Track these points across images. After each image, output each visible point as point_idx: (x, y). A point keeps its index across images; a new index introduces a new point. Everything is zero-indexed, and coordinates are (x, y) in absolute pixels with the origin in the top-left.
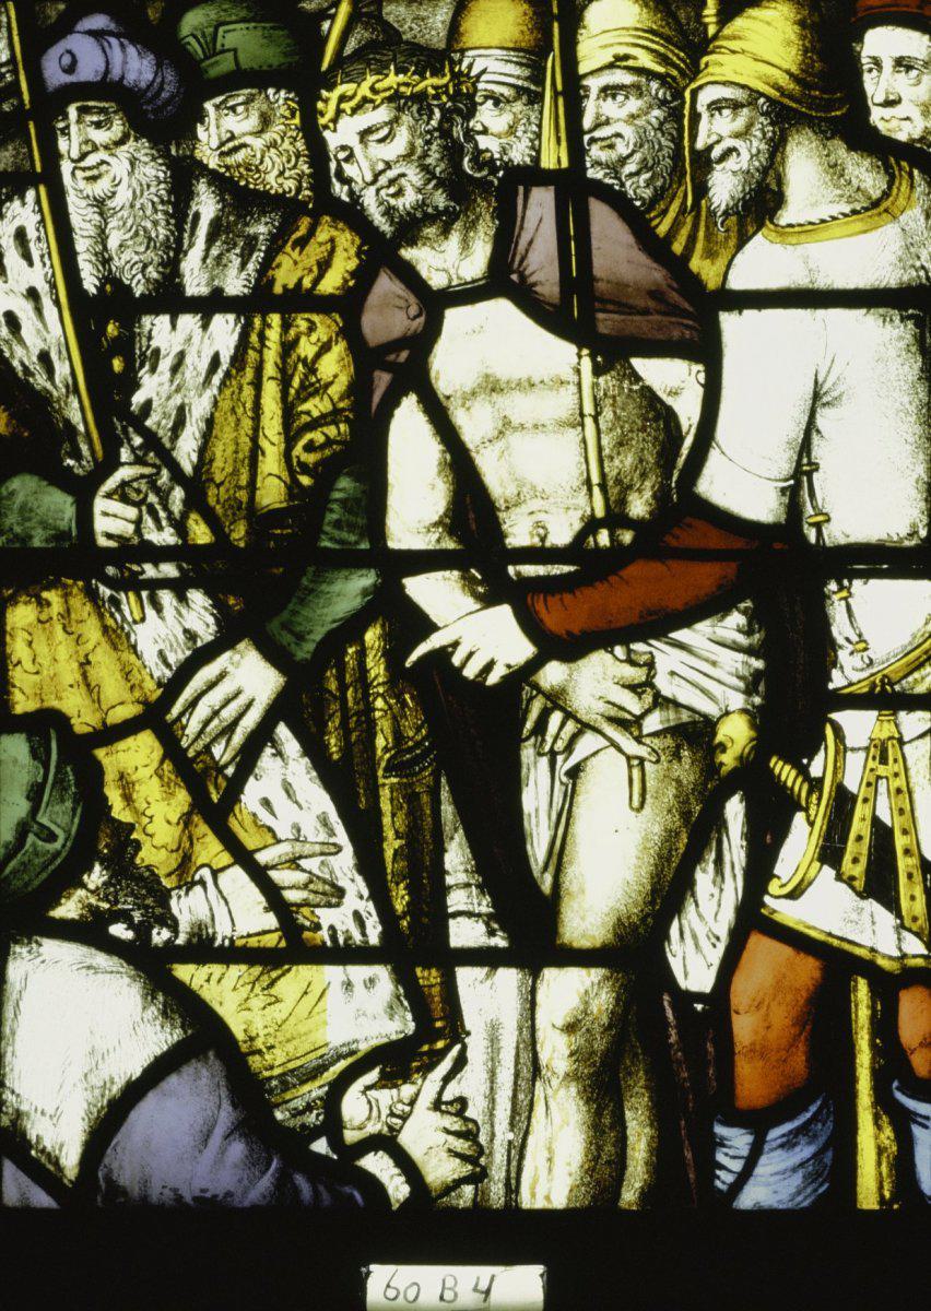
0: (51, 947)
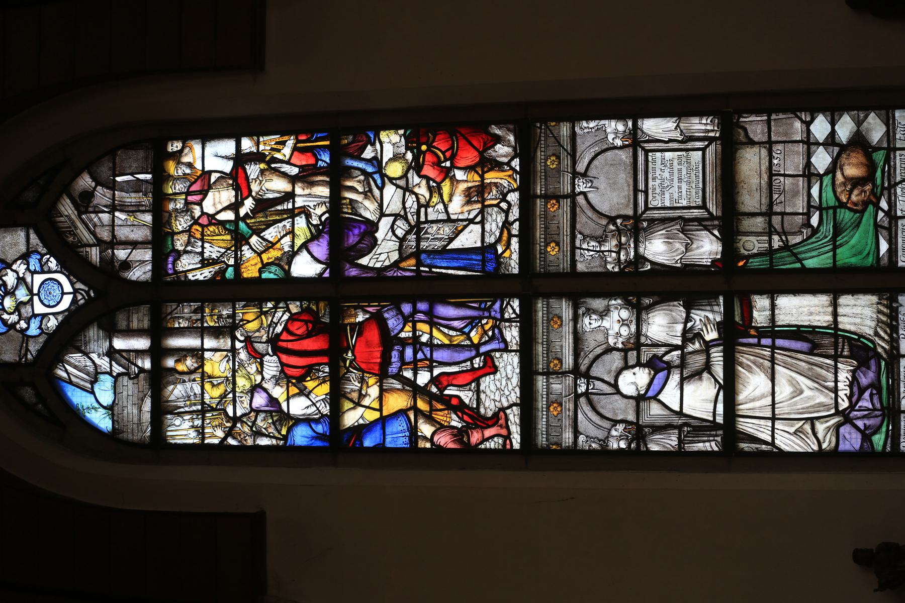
0: (292, 270)
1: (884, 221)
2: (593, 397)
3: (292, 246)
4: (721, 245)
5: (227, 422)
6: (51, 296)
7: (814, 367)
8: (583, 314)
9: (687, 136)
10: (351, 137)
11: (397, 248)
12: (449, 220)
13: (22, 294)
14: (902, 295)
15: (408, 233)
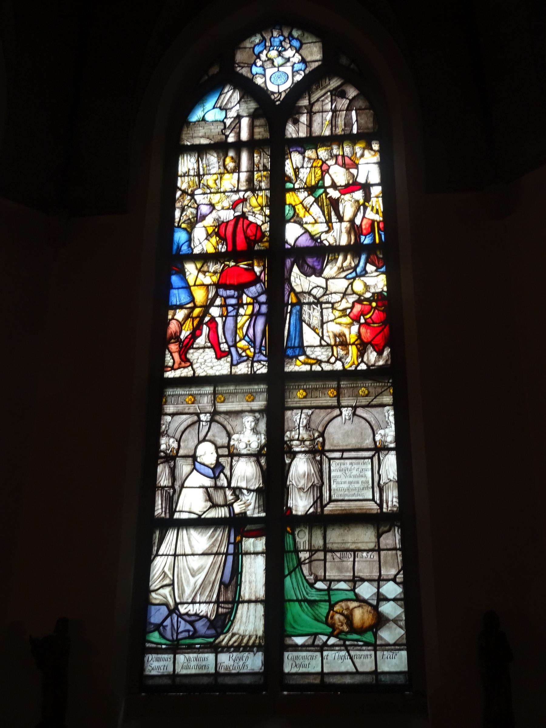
1: (319, 640)
2: (197, 425)
3: (306, 223)
4: (303, 514)
5: (191, 191)
6: (277, 78)
7: (211, 585)
8: (255, 417)
9: (383, 487)
10: (381, 256)
11: (304, 290)
12: (322, 323)
13: (278, 61)
14: (262, 655)
15: (315, 297)
